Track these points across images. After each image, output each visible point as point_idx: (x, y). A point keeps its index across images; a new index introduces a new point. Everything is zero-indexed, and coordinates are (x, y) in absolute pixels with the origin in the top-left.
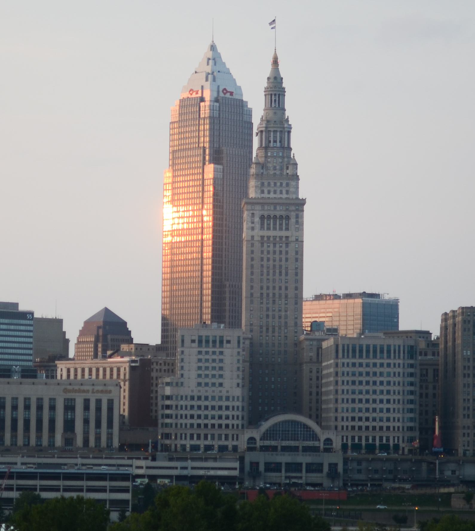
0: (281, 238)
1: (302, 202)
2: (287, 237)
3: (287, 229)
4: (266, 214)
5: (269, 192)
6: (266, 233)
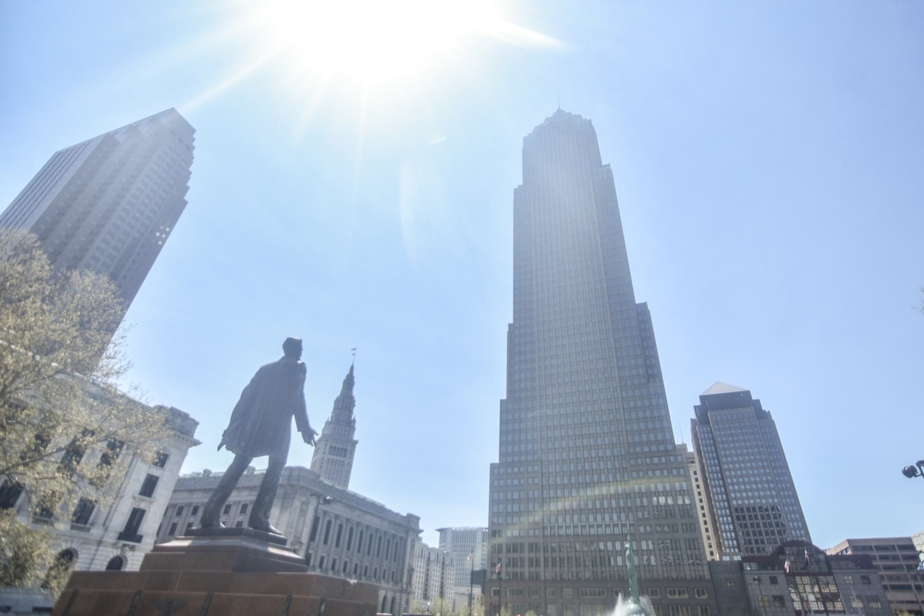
0: (340, 461)
1: (356, 442)
2: (344, 462)
3: (345, 456)
4: (334, 445)
6: (332, 457)
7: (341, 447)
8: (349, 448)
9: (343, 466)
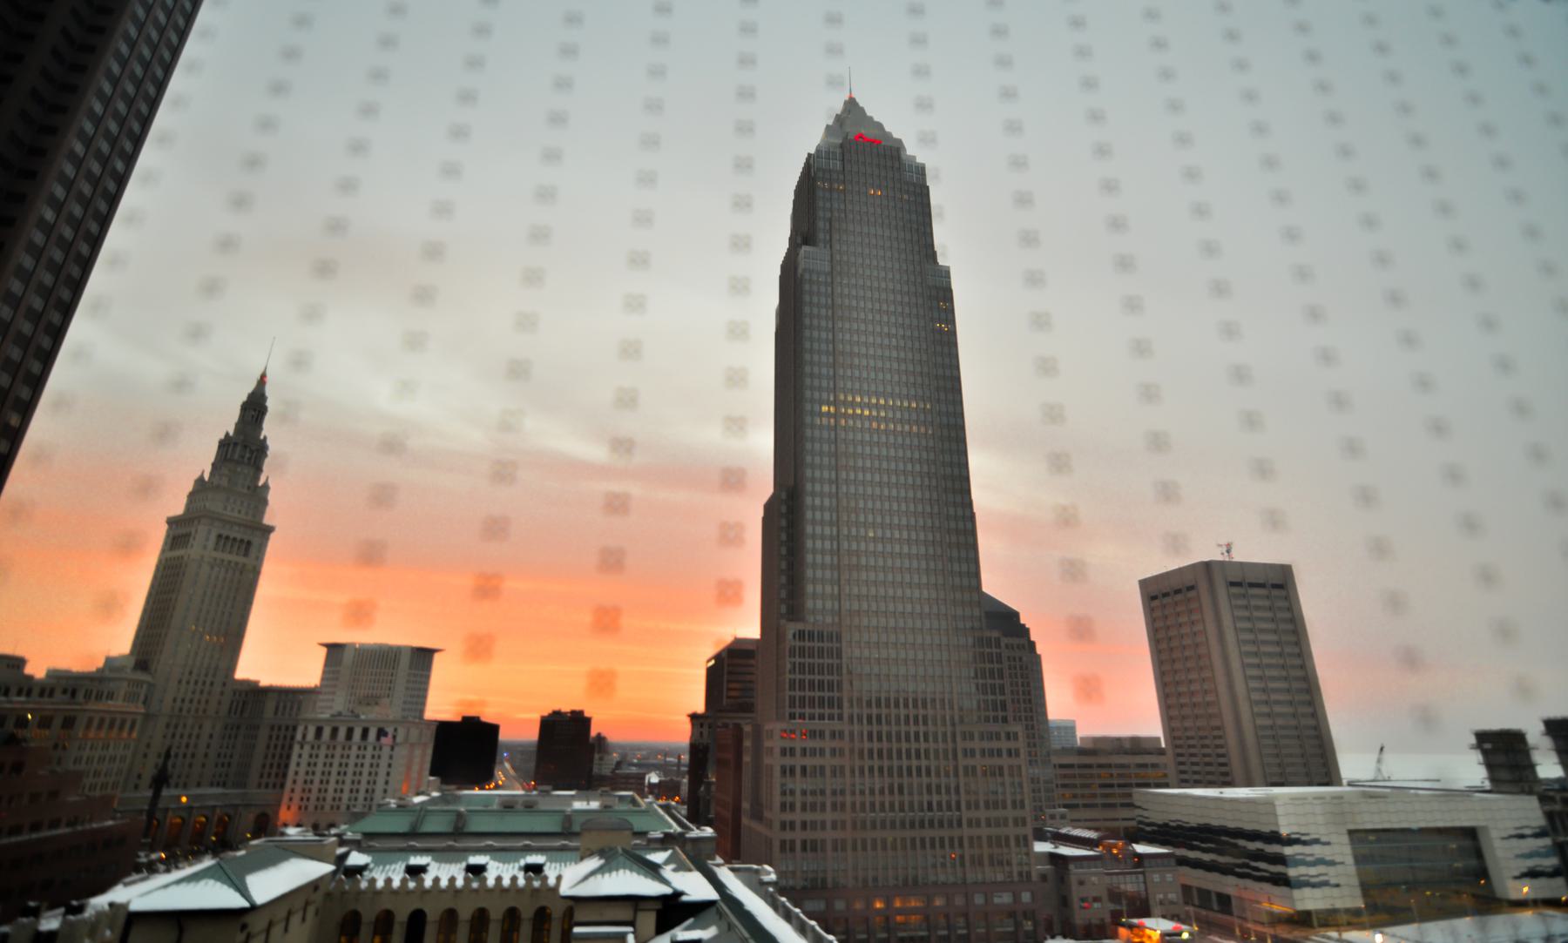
2: (244, 565)
4: (225, 533)
5: (233, 510)
6: (219, 555)
7: (239, 536)
8: (256, 541)
9: (241, 573)
